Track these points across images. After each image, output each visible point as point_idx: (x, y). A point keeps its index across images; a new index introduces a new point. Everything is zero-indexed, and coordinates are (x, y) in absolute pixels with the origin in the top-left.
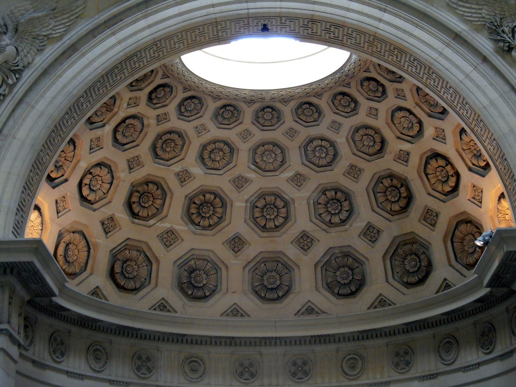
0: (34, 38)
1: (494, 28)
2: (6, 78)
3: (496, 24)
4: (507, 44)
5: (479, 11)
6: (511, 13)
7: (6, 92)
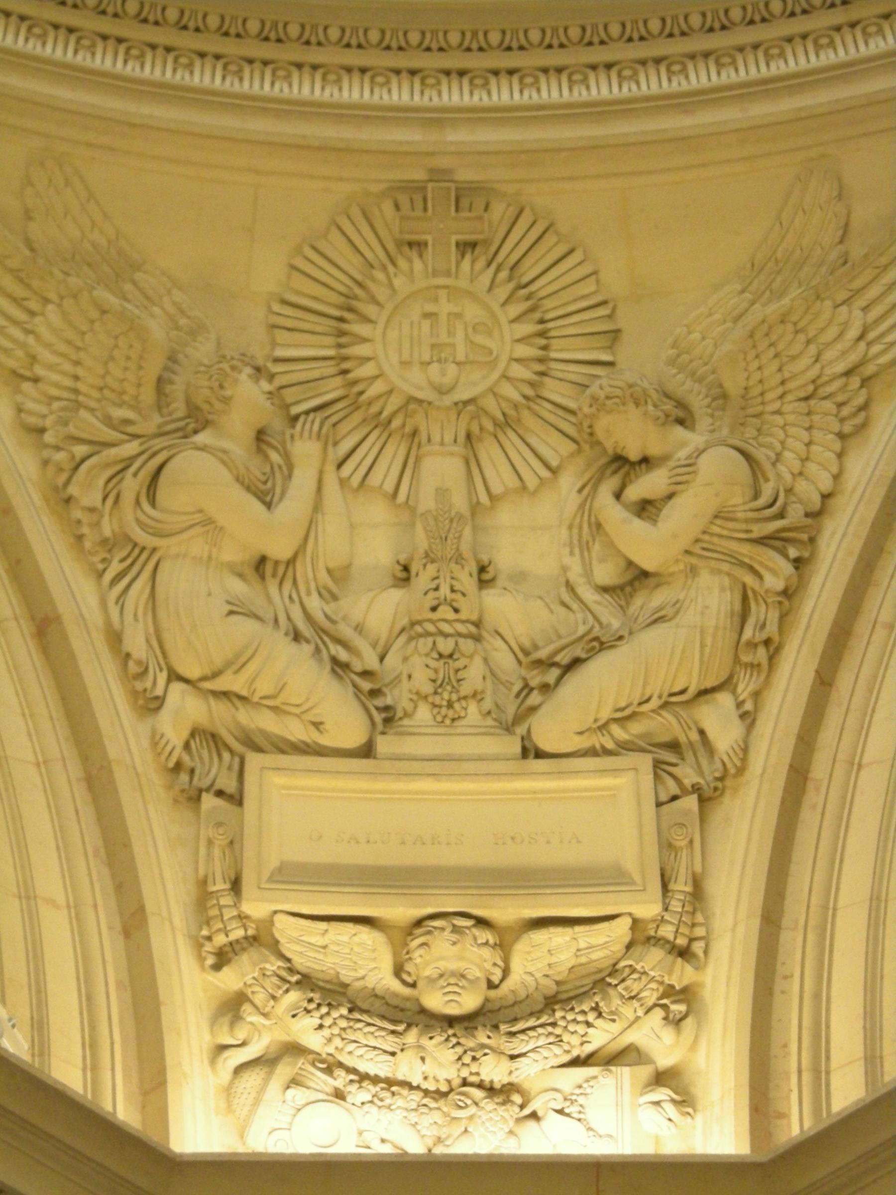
0: (807, 398)
2: (749, 580)
7: (772, 629)
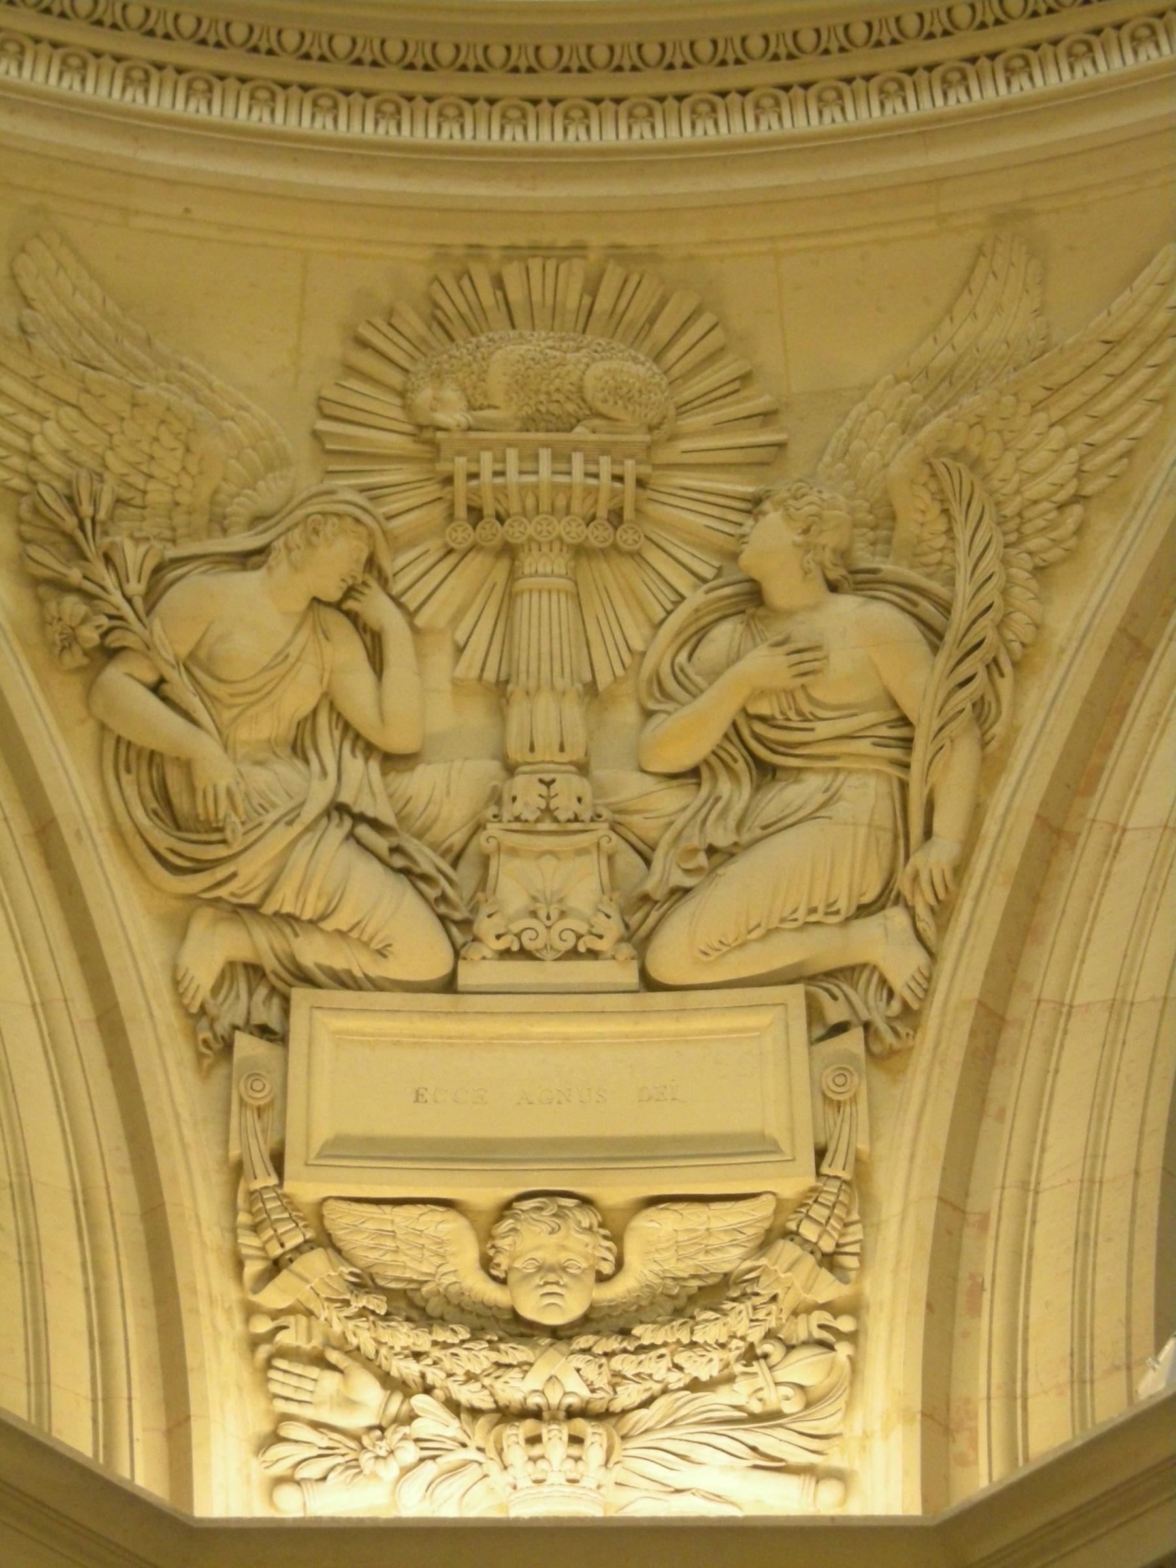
1: (70, 522)
3: (86, 509)
4: (105, 622)
5: (23, 420)
6: (183, 498)
